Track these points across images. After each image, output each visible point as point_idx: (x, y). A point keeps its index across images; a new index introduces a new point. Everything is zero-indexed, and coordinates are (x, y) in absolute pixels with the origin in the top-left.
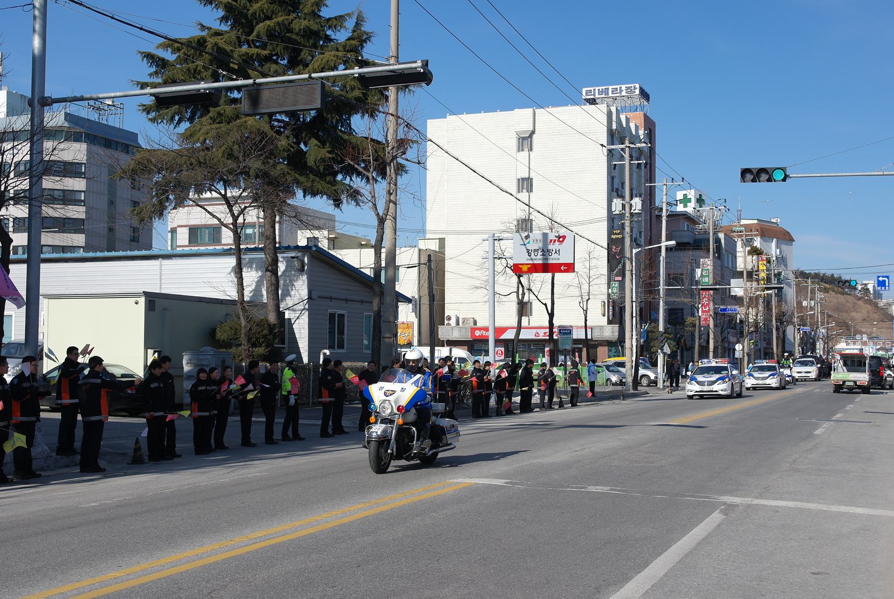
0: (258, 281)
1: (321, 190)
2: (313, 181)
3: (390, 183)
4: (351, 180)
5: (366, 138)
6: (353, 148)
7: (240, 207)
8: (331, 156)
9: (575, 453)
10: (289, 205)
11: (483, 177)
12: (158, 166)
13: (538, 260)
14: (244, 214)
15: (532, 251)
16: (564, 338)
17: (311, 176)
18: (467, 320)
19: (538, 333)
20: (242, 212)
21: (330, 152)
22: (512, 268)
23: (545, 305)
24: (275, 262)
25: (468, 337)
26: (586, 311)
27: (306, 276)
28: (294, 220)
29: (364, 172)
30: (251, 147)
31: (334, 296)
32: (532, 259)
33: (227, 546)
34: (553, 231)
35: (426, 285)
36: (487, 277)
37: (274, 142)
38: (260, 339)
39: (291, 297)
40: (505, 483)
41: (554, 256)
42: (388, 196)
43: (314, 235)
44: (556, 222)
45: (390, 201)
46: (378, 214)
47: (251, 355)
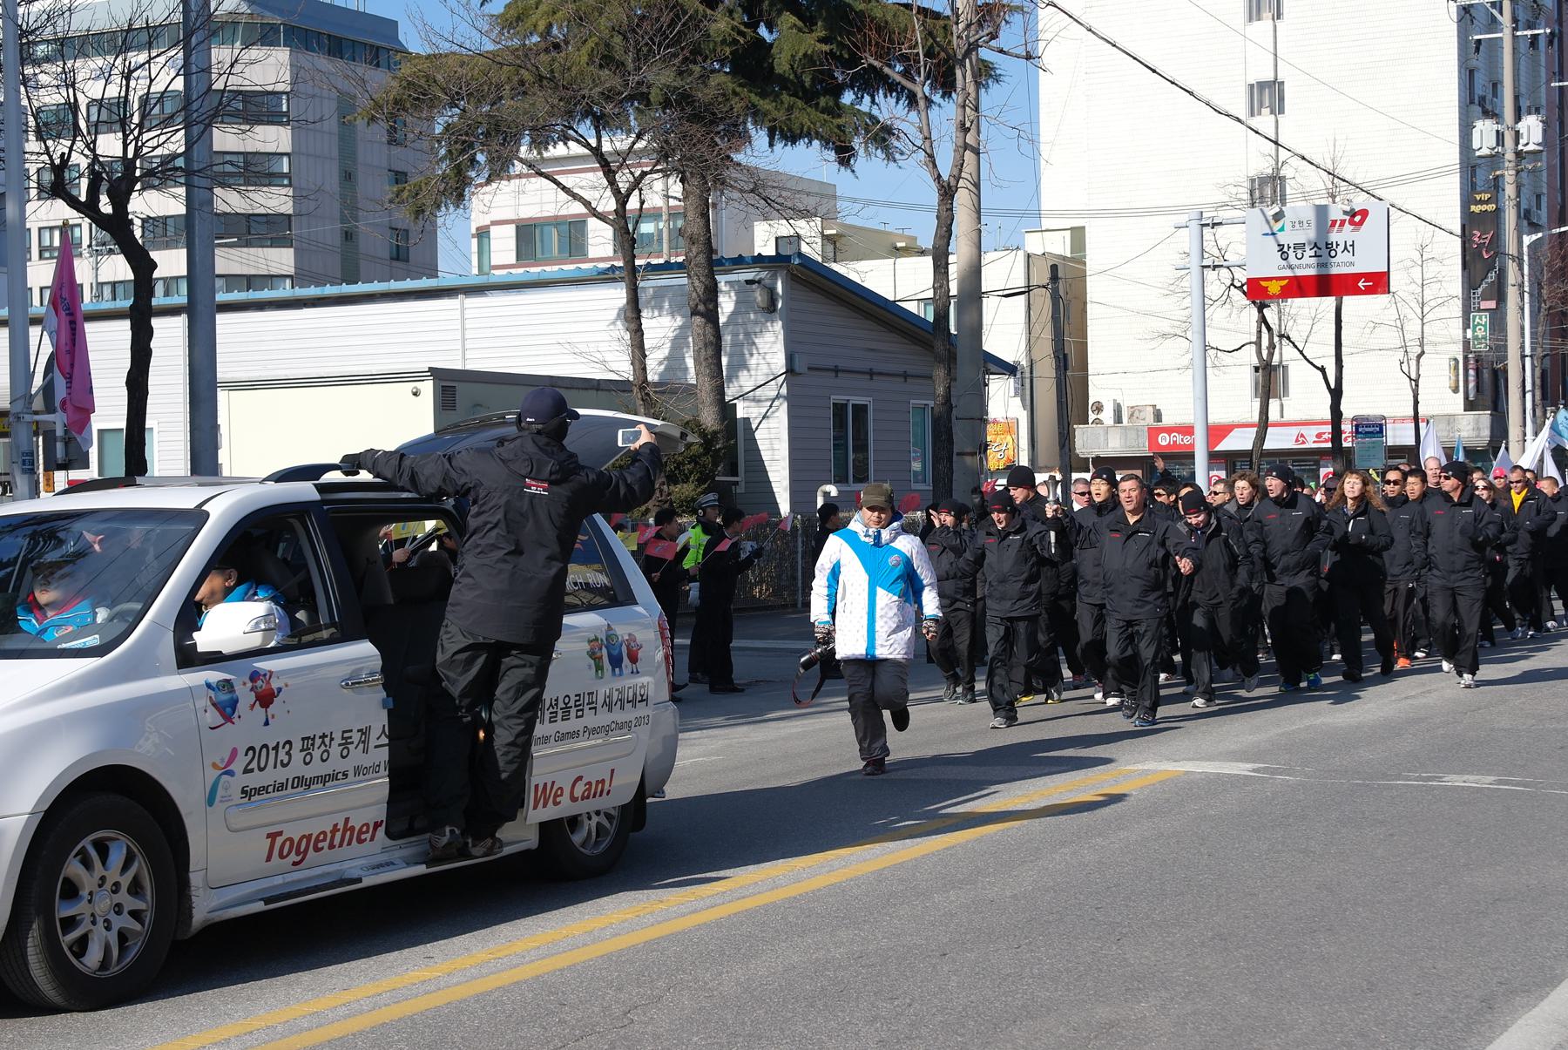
0: (676, 338)
1: (809, 128)
2: (790, 108)
3: (964, 107)
4: (873, 102)
5: (908, 6)
6: (879, 30)
7: (632, 173)
8: (826, 48)
9: (1409, 701)
10: (739, 164)
11: (1173, 83)
12: (451, 90)
13: (1307, 267)
14: (641, 190)
15: (1289, 247)
16: (1367, 445)
17: (785, 97)
18: (1140, 411)
19: (1302, 436)
20: (636, 184)
21: (822, 40)
22: (1245, 288)
23: (1322, 370)
24: (712, 292)
25: (1141, 448)
26: (1417, 381)
27: (780, 323)
28: (752, 198)
29: (905, 82)
30: (651, 39)
31: (842, 364)
32: (1290, 267)
33: (651, 913)
34: (1337, 199)
35: (1047, 335)
36: (1189, 310)
37: (702, 25)
38: (684, 465)
39: (749, 371)
40: (1254, 771)
41: (1342, 257)
42: (961, 135)
43: (798, 230)
44: (1344, 181)
45: (966, 147)
46: (939, 176)
47: (666, 502)
